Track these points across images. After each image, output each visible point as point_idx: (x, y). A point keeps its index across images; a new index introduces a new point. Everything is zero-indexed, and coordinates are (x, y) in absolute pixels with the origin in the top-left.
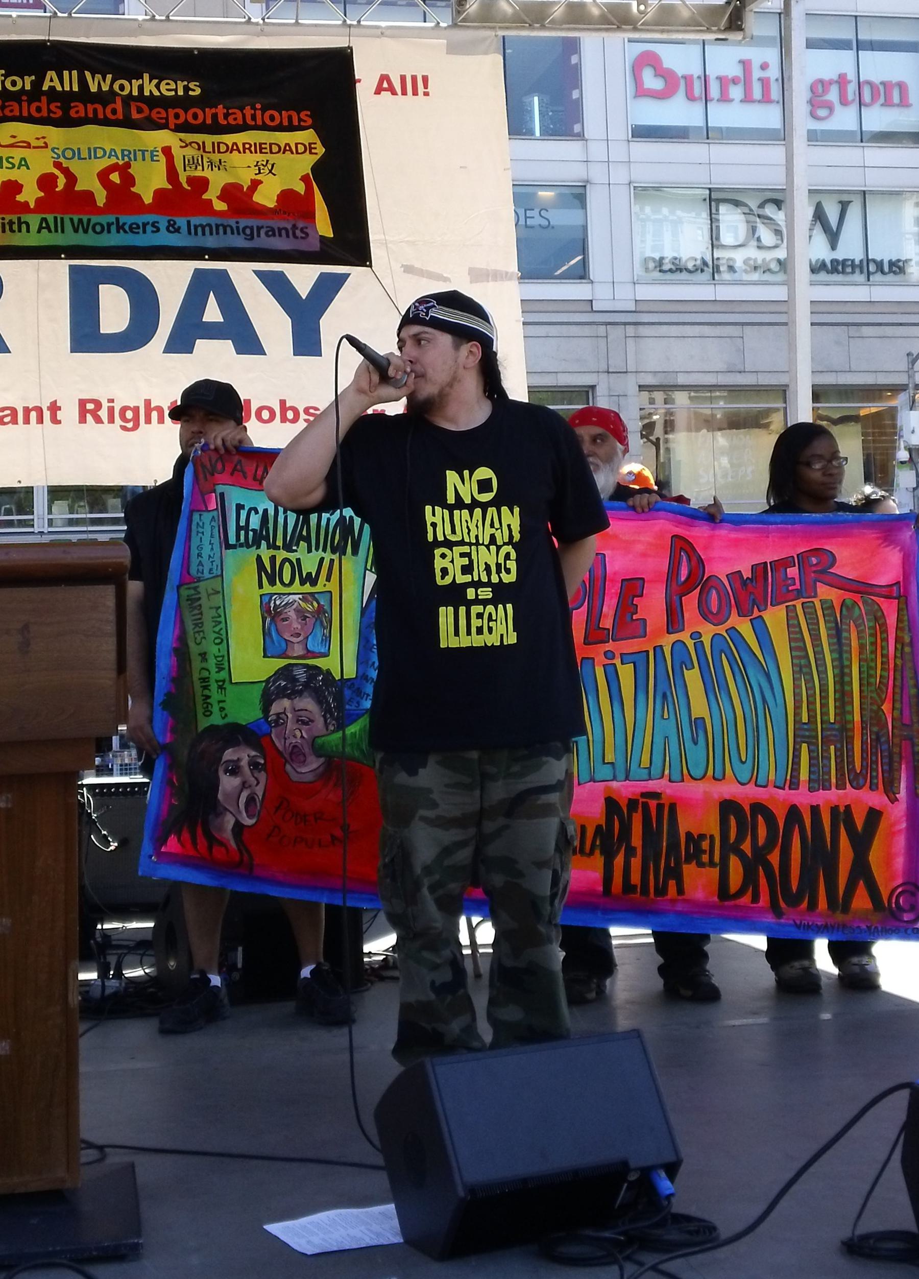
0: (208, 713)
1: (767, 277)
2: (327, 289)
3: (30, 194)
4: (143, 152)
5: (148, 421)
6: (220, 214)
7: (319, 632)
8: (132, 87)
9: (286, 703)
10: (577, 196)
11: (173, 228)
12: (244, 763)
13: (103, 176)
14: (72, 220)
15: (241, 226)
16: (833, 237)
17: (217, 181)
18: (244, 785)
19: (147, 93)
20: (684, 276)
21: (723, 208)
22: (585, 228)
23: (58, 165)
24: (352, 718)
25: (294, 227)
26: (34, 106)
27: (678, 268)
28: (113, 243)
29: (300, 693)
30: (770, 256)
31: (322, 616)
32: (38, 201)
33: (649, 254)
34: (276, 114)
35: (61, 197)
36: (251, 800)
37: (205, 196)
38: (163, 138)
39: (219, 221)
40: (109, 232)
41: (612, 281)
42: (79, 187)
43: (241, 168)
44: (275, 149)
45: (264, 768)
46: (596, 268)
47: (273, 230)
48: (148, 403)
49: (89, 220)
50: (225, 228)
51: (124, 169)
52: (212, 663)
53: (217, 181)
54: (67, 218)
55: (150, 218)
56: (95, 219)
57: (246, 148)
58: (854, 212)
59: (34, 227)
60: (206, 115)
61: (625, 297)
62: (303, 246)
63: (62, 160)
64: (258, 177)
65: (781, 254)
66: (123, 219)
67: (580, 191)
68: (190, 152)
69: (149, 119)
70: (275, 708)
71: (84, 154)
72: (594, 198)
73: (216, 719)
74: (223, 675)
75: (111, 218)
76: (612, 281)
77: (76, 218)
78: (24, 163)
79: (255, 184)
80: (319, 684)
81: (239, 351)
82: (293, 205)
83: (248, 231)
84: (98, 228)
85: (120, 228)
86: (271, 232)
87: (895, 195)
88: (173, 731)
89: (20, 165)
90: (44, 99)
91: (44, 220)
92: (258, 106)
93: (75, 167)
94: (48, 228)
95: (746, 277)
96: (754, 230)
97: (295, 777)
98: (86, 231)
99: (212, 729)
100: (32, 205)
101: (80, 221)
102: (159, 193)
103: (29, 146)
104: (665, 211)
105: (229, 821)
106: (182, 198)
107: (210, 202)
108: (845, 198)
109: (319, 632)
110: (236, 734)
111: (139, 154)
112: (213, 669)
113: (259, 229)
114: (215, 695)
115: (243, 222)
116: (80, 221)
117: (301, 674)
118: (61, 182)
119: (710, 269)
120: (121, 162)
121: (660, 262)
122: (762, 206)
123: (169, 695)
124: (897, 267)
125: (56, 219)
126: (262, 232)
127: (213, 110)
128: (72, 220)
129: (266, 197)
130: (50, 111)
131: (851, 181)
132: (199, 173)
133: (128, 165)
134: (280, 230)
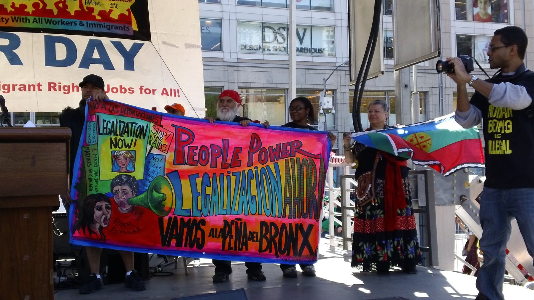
0: (91, 190)
1: (280, 53)
2: (136, 48)
3: (30, 9)
7: (131, 164)
9: (119, 187)
10: (219, 23)
12: (104, 206)
13: (56, 4)
14: (45, 19)
15: (106, 25)
16: (301, 41)
17: (97, 9)
18: (103, 214)
20: (253, 51)
21: (267, 30)
22: (221, 34)
24: (142, 193)
25: (124, 26)
27: (251, 49)
29: (124, 184)
30: (281, 46)
31: (132, 159)
32: (33, 12)
33: (241, 43)
36: (106, 219)
39: (98, 23)
40: (59, 24)
41: (230, 52)
42: (47, 8)
45: (111, 208)
46: (225, 48)
47: (117, 27)
48: (73, 84)
50: (100, 25)
52: (93, 173)
53: (97, 9)
56: (53, 19)
58: (308, 33)
59: (31, 21)
61: (234, 57)
62: (127, 33)
64: (112, 9)
65: (285, 46)
66: (64, 20)
67: (220, 21)
70: (115, 189)
72: (225, 24)
73: (94, 192)
74: (97, 177)
75: (60, 19)
76: (230, 52)
77: (46, 18)
79: (111, 11)
80: (131, 181)
83: (108, 27)
84: (55, 23)
86: (116, 28)
87: (320, 27)
88: (78, 196)
91: (35, 19)
95: (272, 52)
96: (276, 37)
97: (121, 211)
99: (93, 196)
100: (31, 13)
101: (48, 20)
102: (76, 12)
104: (247, 30)
105: (98, 226)
107: (95, 16)
108: (305, 28)
109: (131, 164)
110: (101, 197)
112: (94, 175)
113: (112, 26)
114: (94, 184)
115: (107, 24)
116: (48, 20)
117: (124, 178)
118: (41, 6)
119: (261, 49)
121: (245, 47)
122: (279, 29)
123: (77, 184)
124: (321, 51)
125: (39, 19)
126: (113, 28)
128: (45, 19)
131: (307, 22)
134: (119, 27)
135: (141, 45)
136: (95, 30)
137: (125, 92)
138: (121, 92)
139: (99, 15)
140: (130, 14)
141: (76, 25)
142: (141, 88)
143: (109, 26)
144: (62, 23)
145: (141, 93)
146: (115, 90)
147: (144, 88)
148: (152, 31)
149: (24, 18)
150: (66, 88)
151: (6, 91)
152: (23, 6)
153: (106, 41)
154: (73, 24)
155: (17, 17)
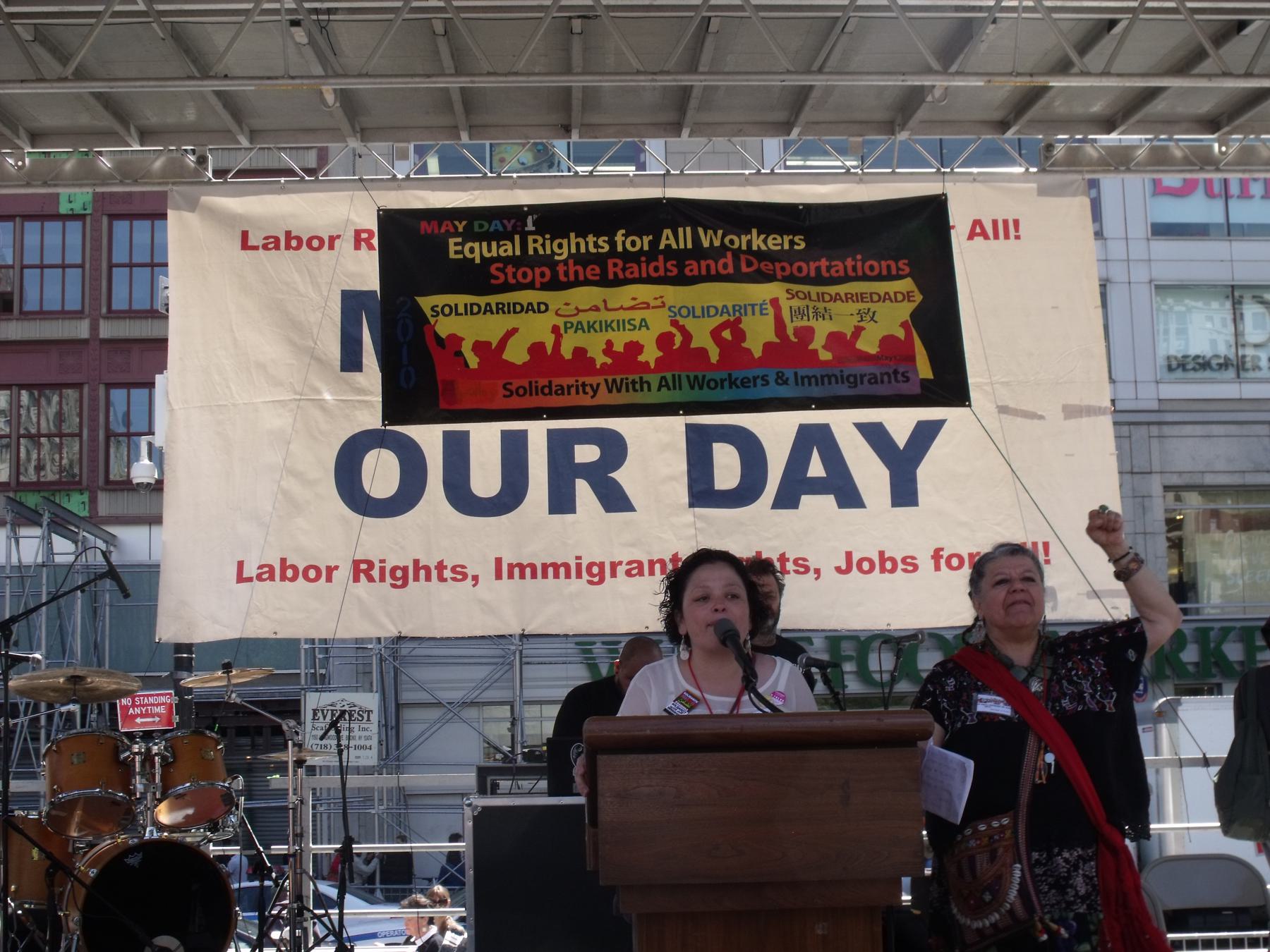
2: (925, 434)
3: (651, 354)
4: (753, 306)
6: (826, 363)
8: (740, 242)
14: (688, 377)
17: (822, 329)
19: (755, 248)
23: (674, 323)
25: (896, 372)
26: (652, 265)
28: (725, 398)
32: (658, 360)
34: (875, 264)
35: (678, 353)
37: (811, 347)
40: (722, 387)
42: (693, 345)
43: (843, 318)
44: (875, 298)
49: (704, 377)
51: (734, 325)
53: (822, 329)
54: (684, 375)
57: (849, 297)
59: (655, 386)
60: (810, 268)
63: (678, 318)
64: (861, 324)
68: (796, 303)
69: (758, 271)
71: (698, 312)
78: (644, 324)
79: (858, 331)
81: (841, 505)
82: (895, 351)
83: (852, 379)
84: (712, 384)
89: (641, 326)
90: (661, 258)
91: (663, 378)
92: (859, 257)
93: (689, 324)
94: (667, 386)
98: (701, 388)
100: (652, 365)
101: (696, 377)
102: (768, 346)
107: (815, 352)
111: (749, 309)
120: (732, 319)
127: (817, 264)
128: (688, 377)
129: (868, 344)
130: (666, 270)
132: (805, 323)
133: (738, 320)
135: (939, 424)
136: (816, 391)
137: (893, 570)
138: (883, 570)
139: (825, 347)
141: (767, 383)
143: (855, 376)
144: (732, 383)
145: (937, 568)
146: (866, 566)
147: (945, 554)
148: (972, 380)
149: (637, 380)
151: (596, 579)
153: (843, 423)
154: (759, 382)
155: (618, 379)
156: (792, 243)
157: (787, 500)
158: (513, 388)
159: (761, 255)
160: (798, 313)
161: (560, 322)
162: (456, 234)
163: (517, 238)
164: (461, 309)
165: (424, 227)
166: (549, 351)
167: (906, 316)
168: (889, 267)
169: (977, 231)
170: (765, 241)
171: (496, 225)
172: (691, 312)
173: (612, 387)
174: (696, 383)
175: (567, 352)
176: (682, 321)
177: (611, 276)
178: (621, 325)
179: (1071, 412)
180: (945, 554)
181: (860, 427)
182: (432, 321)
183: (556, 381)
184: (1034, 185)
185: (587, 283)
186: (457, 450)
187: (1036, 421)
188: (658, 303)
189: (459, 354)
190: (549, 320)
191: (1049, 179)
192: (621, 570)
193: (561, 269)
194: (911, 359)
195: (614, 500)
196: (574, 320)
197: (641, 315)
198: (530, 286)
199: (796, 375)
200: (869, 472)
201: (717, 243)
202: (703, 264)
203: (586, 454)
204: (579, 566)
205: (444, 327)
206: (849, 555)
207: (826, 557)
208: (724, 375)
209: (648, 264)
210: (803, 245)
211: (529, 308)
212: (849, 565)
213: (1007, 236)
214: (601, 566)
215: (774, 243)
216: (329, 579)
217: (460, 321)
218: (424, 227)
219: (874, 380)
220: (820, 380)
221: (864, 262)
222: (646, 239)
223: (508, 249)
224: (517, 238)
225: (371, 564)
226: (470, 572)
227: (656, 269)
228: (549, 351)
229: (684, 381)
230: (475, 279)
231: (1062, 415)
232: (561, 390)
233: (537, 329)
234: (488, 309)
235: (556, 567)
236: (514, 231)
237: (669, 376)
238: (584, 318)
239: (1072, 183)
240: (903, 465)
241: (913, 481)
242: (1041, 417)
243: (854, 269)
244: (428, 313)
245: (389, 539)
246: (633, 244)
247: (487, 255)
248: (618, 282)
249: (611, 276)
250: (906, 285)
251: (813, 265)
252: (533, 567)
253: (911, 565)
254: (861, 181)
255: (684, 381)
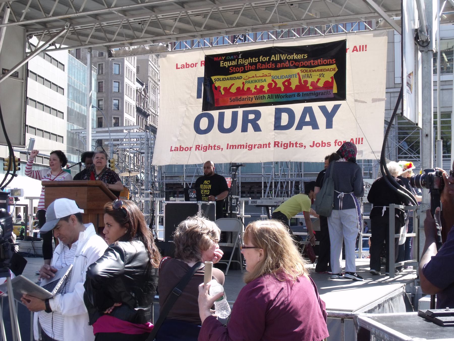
2: (336, 108)
5: (290, 146)
6: (311, 90)
8: (291, 57)
11: (299, 95)
17: (310, 80)
23: (273, 81)
32: (268, 90)
35: (273, 89)
37: (307, 86)
38: (298, 70)
42: (278, 86)
44: (325, 70)
53: (310, 80)
54: (274, 95)
55: (294, 93)
59: (267, 98)
60: (308, 63)
68: (303, 74)
85: (286, 97)
91: (269, 95)
93: (277, 81)
103: (266, 76)
106: (302, 87)
107: (308, 87)
118: (274, 85)
136: (307, 98)
138: (322, 146)
140: (332, 81)
142: (335, 142)
145: (335, 145)
146: (318, 145)
150: (286, 145)
152: (262, 87)
153: (315, 106)
156: (304, 56)
157: (299, 127)
158: (232, 99)
159: (296, 61)
160: (304, 76)
161: (244, 81)
162: (222, 60)
163: (236, 60)
164: (221, 79)
165: (215, 59)
166: (241, 89)
167: (333, 75)
168: (330, 61)
169: (355, 49)
170: (297, 56)
171: (232, 57)
172: (278, 77)
173: (257, 98)
174: (277, 97)
175: (245, 89)
176: (275, 80)
177: (258, 68)
178: (259, 81)
179: (374, 100)
180: (338, 141)
181: (320, 107)
182: (214, 83)
183: (243, 97)
184: (372, 34)
185: (252, 70)
186: (222, 116)
187: (364, 104)
188: (269, 75)
189: (220, 91)
190: (242, 80)
191: (377, 32)
192: (256, 146)
193: (246, 67)
194: (332, 87)
195: (257, 128)
196: (248, 80)
197: (264, 78)
198: (239, 72)
199: (305, 94)
200: (321, 119)
201: (285, 59)
202: (282, 64)
203: (251, 117)
204: (246, 145)
205: (217, 84)
206: (314, 142)
207: (307, 142)
208: (285, 94)
209: (267, 64)
210: (307, 57)
211: (238, 78)
212: (314, 145)
213: (363, 50)
214: (252, 145)
215: (300, 57)
216: (190, 150)
217: (220, 82)
218: (215, 59)
219: (322, 94)
220: (308, 95)
221: (323, 60)
222: (268, 58)
223: (234, 63)
224: (236, 60)
225: (199, 146)
226: (221, 147)
227: (269, 66)
228: (241, 89)
229: (274, 96)
230: (226, 72)
231: (371, 101)
232: (244, 99)
233: (238, 83)
234: (228, 79)
235: (241, 146)
236: (236, 58)
237: (270, 95)
238: (250, 80)
239: (383, 32)
240: (330, 116)
241: (332, 121)
242: (366, 102)
243: (320, 62)
244: (214, 80)
245: (202, 140)
246: (264, 59)
247: (229, 65)
248: (259, 70)
249: (258, 68)
250: (334, 66)
251: (309, 62)
252: (236, 146)
253: (329, 144)
254: (324, 37)
255: (274, 96)
